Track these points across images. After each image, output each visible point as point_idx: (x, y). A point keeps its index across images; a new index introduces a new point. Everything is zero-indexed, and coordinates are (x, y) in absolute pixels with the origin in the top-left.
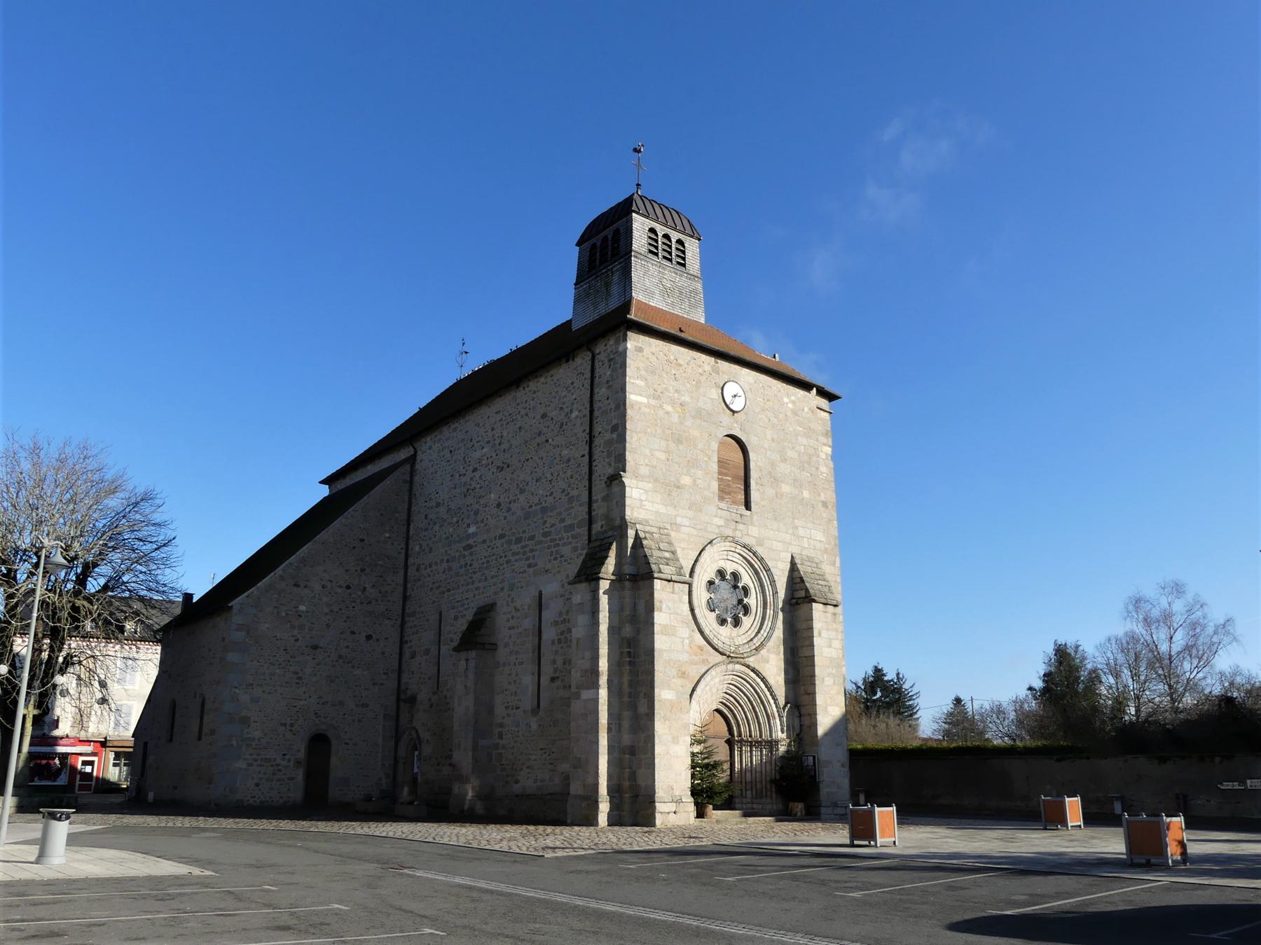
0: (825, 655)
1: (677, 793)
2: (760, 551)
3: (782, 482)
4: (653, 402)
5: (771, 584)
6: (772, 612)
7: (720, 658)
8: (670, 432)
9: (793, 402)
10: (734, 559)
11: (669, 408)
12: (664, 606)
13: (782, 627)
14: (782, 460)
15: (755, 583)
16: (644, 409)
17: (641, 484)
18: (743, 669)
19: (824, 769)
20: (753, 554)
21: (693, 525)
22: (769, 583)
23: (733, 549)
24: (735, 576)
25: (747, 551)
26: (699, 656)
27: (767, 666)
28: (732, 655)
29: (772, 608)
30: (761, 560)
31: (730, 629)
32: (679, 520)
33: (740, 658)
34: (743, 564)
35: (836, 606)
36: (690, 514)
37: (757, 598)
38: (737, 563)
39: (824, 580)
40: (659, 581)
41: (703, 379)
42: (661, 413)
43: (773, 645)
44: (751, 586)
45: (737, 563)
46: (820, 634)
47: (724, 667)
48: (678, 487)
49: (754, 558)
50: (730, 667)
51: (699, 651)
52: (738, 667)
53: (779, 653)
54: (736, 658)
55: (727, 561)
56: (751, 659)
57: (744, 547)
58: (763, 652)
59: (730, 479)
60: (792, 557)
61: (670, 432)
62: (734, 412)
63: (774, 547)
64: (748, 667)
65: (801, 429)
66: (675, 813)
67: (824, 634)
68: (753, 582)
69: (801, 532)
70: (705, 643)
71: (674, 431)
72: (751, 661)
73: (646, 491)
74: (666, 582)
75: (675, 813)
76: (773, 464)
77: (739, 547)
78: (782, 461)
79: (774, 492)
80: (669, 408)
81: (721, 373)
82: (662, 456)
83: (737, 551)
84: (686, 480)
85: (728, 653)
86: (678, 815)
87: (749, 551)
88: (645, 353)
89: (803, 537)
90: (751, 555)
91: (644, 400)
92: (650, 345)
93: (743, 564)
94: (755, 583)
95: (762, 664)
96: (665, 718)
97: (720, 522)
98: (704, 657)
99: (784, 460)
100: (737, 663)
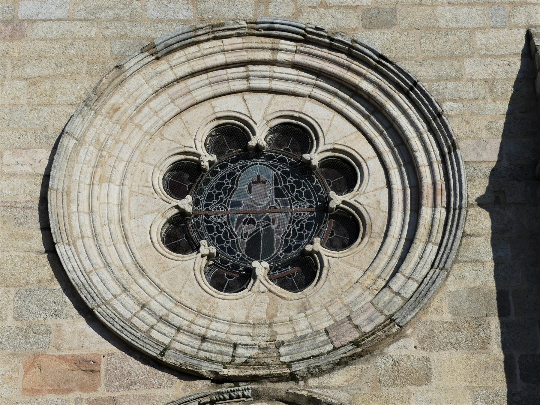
5: (431, 130)
6: (441, 213)
13: (490, 256)
15: (379, 141)
20: (350, 54)
21: (82, 15)
22: (423, 127)
23: (267, 55)
25: (324, 52)
26: (77, 394)
28: (225, 372)
29: (442, 199)
31: (267, 298)
33: (280, 378)
34: (318, 93)
37: (389, 184)
38: (294, 94)
43: (448, 317)
45: (294, 94)
49: (356, 65)
51: (79, 375)
53: (484, 345)
54: (254, 379)
55: (247, 96)
57: (307, 41)
60: (529, 36)
63: (442, 23)
68: (370, 140)
70: (108, 347)
77: (284, 44)
83: (281, 56)
85: (205, 368)
87: (331, 48)
90: (342, 58)
93: (318, 93)
94: (379, 141)
95: (392, 391)
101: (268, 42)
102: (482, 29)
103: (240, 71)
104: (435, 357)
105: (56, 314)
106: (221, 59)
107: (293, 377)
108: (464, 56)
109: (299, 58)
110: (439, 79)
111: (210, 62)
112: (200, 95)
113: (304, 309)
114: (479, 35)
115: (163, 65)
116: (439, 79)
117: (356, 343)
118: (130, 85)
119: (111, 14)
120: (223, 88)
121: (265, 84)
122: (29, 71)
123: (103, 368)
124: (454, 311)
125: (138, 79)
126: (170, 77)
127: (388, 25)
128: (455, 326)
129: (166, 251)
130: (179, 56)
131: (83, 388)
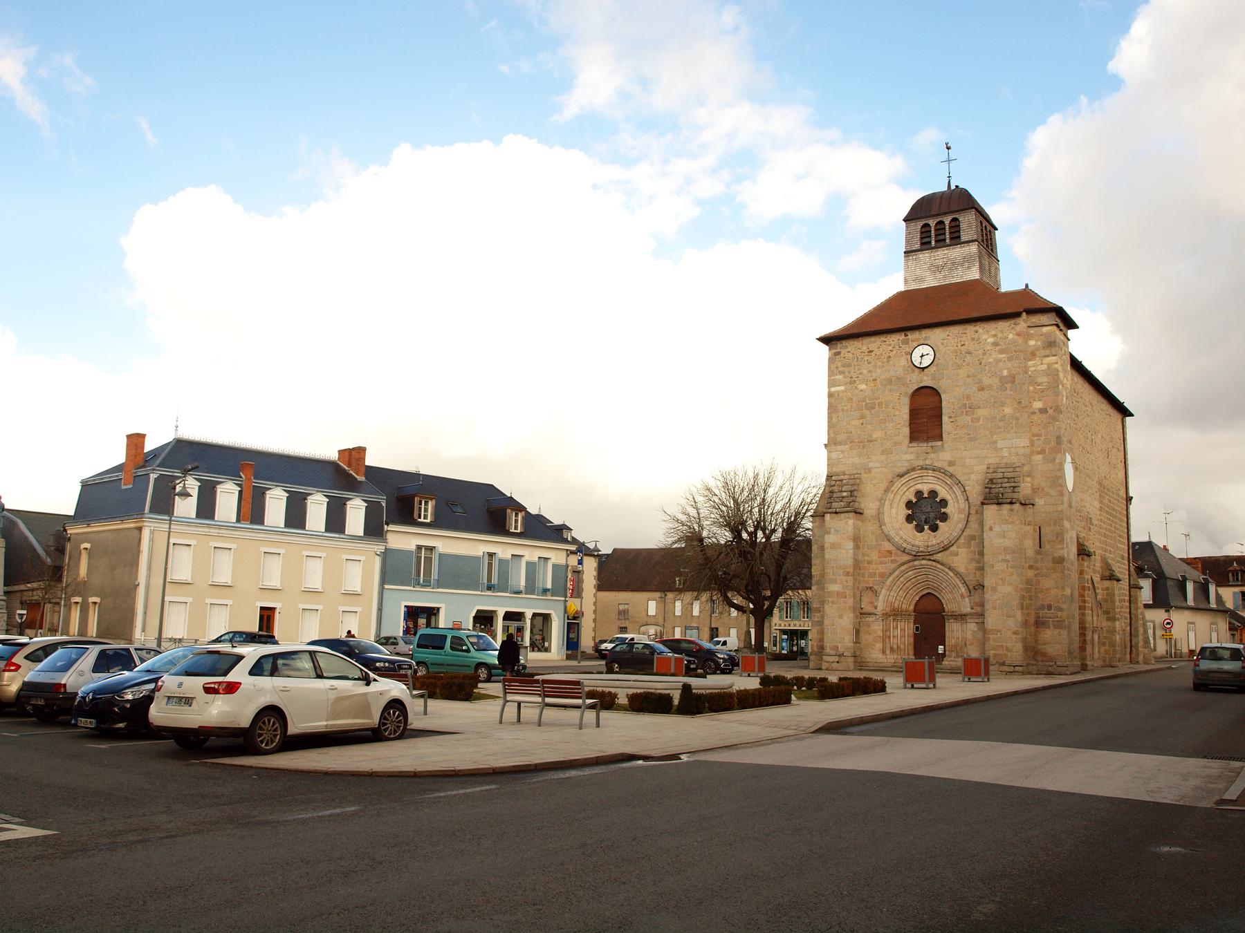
0: (996, 545)
1: (841, 650)
2: (951, 469)
3: (979, 407)
4: (849, 387)
7: (906, 558)
8: (864, 403)
9: (995, 336)
10: (930, 481)
11: (863, 387)
12: (832, 530)
14: (979, 390)
16: (841, 395)
17: (839, 448)
18: (930, 563)
19: (991, 636)
23: (926, 474)
24: (933, 493)
27: (956, 558)
30: (951, 476)
32: (871, 465)
35: (1011, 503)
36: (883, 457)
39: (1014, 482)
40: (829, 515)
41: (892, 354)
42: (856, 392)
44: (948, 497)
46: (991, 529)
47: (911, 564)
48: (872, 441)
50: (917, 563)
51: (888, 554)
52: (924, 562)
56: (939, 555)
58: (953, 549)
59: (926, 420)
61: (864, 403)
62: (923, 369)
64: (934, 561)
65: (1004, 356)
66: (838, 662)
67: (997, 528)
69: (1000, 444)
71: (868, 401)
72: (939, 557)
73: (843, 452)
74: (835, 515)
75: (838, 662)
76: (968, 397)
78: (979, 390)
79: (969, 418)
80: (863, 387)
81: (910, 343)
82: (857, 423)
84: (878, 434)
86: (840, 664)
88: (842, 354)
89: (1002, 449)
91: (842, 388)
92: (846, 347)
96: (833, 603)
97: (908, 457)
98: (893, 558)
99: (981, 389)
100: (923, 559)
101: (926, 471)
102: (976, 466)
103: (920, 478)
104: (960, 550)
105: (883, 541)
106: (916, 476)
107: (930, 555)
108: (972, 473)
109: (933, 475)
110: (966, 480)
111: (913, 477)
112: (912, 484)
113: (935, 537)
114: (975, 467)
115: (902, 479)
116: (966, 480)
117: (943, 547)
118: (895, 485)
119: (890, 465)
120: (917, 482)
121: (926, 481)
122: (873, 482)
123: (893, 552)
124: (965, 540)
125: (897, 483)
126: (904, 481)
127: (954, 465)
128: (964, 543)
129: (906, 524)
130: (905, 477)
131: (890, 557)
